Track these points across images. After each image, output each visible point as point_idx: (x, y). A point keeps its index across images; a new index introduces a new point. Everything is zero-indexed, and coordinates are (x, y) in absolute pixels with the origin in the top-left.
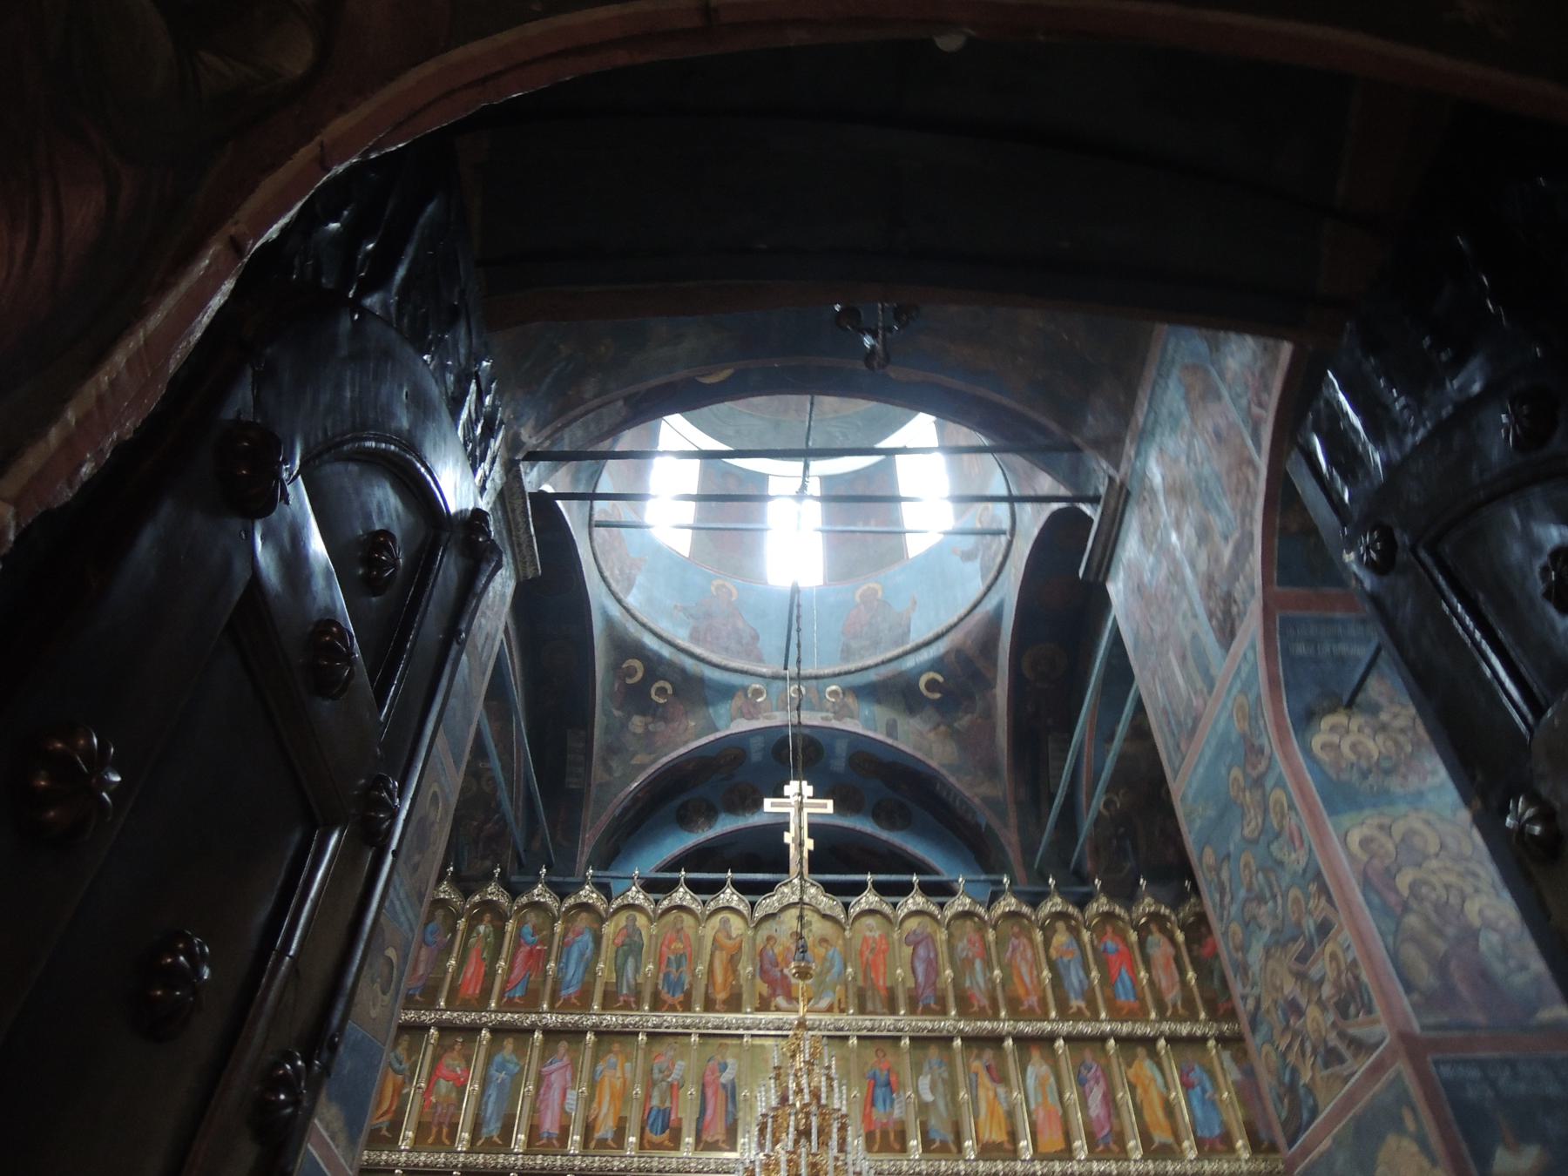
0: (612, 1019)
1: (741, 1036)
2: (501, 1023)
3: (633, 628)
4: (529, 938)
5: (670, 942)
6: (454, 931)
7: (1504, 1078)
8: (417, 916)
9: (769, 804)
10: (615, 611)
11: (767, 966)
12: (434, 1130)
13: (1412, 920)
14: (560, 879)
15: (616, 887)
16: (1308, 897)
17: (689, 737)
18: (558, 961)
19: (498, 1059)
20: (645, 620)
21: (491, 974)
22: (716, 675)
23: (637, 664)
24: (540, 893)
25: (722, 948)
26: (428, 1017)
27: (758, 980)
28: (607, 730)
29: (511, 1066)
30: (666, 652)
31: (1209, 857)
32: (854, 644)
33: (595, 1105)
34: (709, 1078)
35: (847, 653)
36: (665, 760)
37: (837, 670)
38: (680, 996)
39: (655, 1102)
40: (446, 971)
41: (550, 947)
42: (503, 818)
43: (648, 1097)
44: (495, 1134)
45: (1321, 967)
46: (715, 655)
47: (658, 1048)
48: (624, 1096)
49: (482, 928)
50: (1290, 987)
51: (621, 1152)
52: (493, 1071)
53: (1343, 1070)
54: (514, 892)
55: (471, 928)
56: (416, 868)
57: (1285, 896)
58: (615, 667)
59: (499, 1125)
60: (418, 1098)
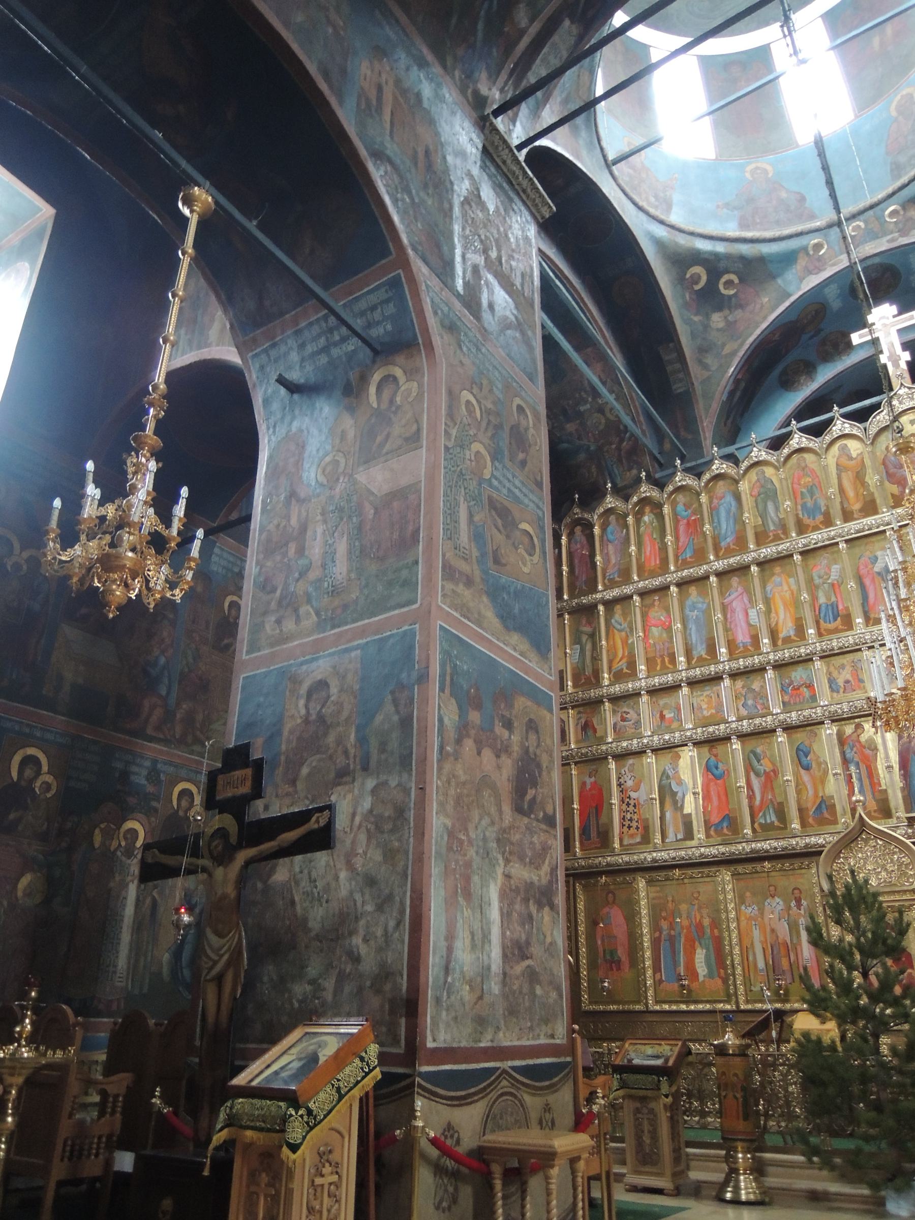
0: (768, 551)
1: (884, 531)
2: (682, 578)
3: (683, 241)
4: (684, 513)
5: (799, 480)
6: (626, 526)
8: (541, 499)
9: (856, 338)
10: (661, 232)
11: (892, 470)
12: (659, 661)
14: (693, 463)
15: (740, 455)
17: (766, 312)
18: (711, 522)
19: (688, 603)
20: (691, 228)
21: (664, 548)
22: (774, 248)
23: (697, 269)
24: (680, 479)
25: (846, 469)
26: (627, 590)
27: (887, 484)
28: (693, 336)
29: (700, 605)
30: (720, 248)
32: (902, 159)
33: (773, 615)
34: (863, 572)
35: (897, 169)
36: (751, 339)
37: (890, 190)
38: (820, 518)
39: (822, 600)
40: (630, 555)
41: (702, 515)
42: (632, 435)
43: (814, 598)
44: (703, 653)
46: (768, 230)
47: (811, 562)
48: (797, 603)
49: (646, 518)
51: (805, 642)
52: (687, 612)
54: (660, 485)
55: (638, 521)
56: (523, 463)
58: (681, 280)
59: (704, 646)
60: (641, 644)
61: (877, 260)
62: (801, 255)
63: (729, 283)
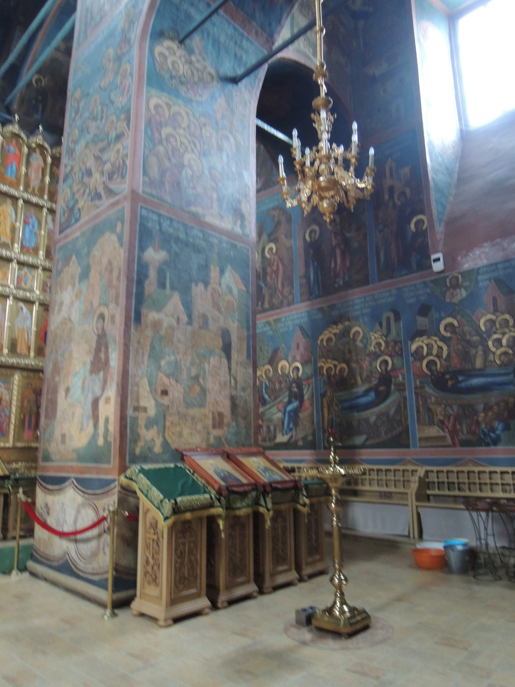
7: (165, 225)
13: (161, 149)
16: (118, 119)
31: (78, 94)
45: (110, 156)
50: (91, 163)
53: (97, 202)
57: (107, 118)
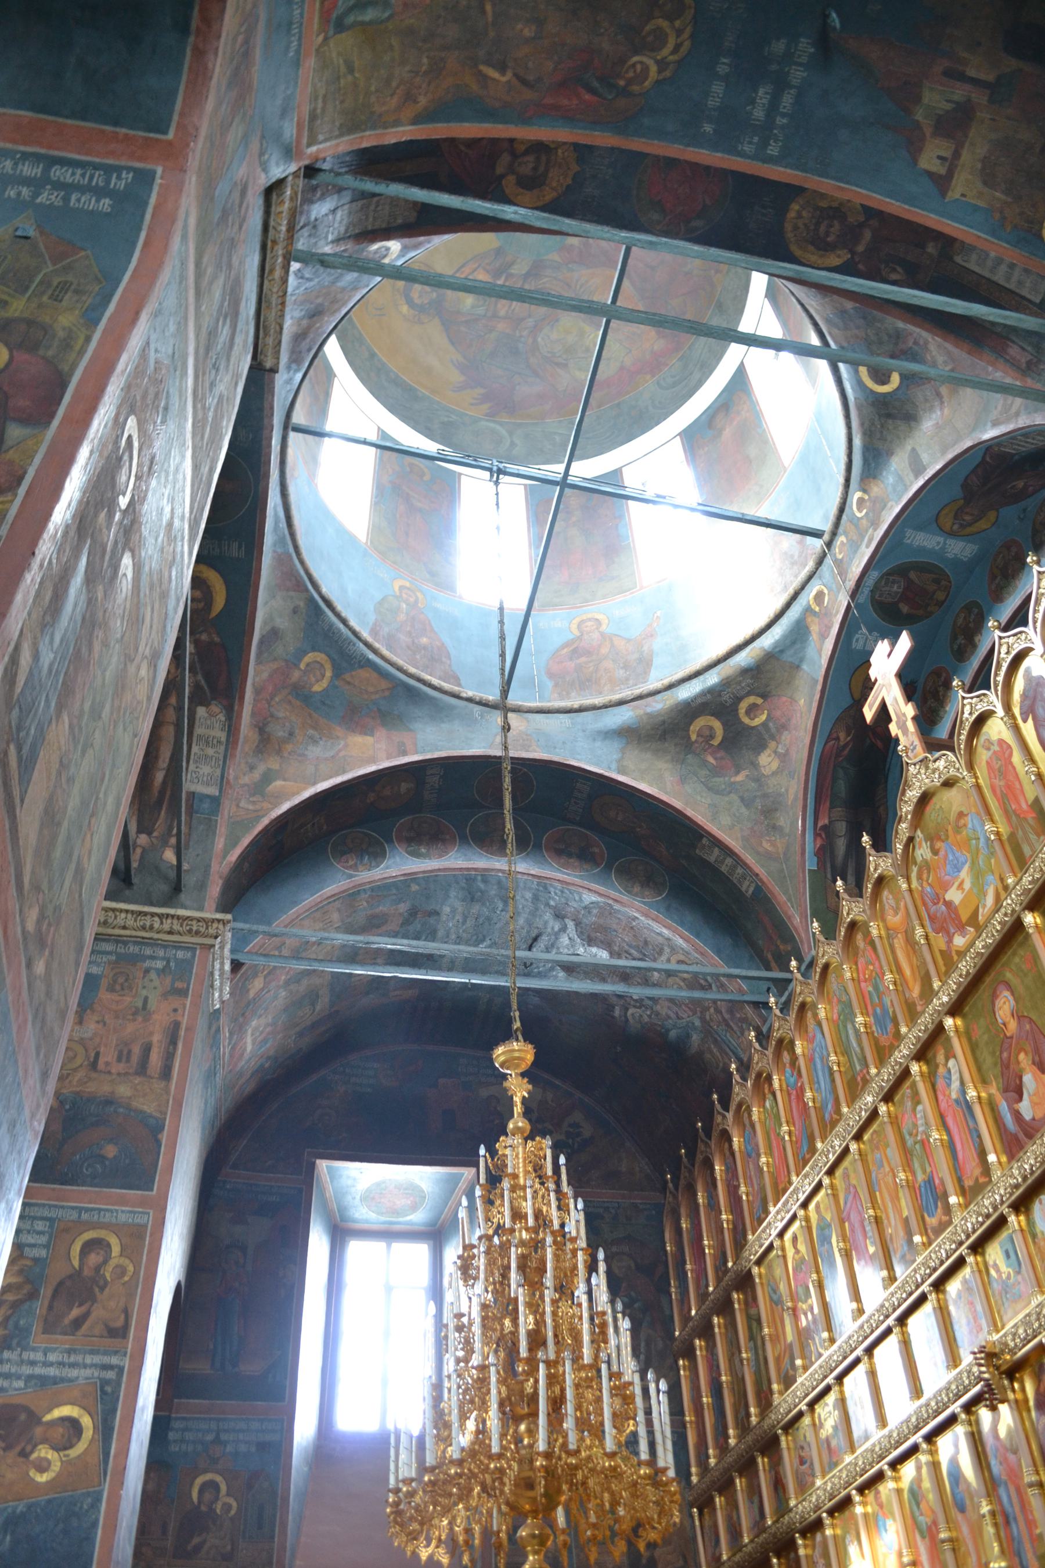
22: (777, 632)
30: (712, 679)
61: (874, 575)
62: (809, 620)
63: (752, 710)
